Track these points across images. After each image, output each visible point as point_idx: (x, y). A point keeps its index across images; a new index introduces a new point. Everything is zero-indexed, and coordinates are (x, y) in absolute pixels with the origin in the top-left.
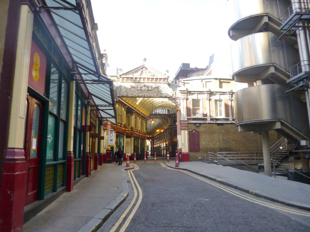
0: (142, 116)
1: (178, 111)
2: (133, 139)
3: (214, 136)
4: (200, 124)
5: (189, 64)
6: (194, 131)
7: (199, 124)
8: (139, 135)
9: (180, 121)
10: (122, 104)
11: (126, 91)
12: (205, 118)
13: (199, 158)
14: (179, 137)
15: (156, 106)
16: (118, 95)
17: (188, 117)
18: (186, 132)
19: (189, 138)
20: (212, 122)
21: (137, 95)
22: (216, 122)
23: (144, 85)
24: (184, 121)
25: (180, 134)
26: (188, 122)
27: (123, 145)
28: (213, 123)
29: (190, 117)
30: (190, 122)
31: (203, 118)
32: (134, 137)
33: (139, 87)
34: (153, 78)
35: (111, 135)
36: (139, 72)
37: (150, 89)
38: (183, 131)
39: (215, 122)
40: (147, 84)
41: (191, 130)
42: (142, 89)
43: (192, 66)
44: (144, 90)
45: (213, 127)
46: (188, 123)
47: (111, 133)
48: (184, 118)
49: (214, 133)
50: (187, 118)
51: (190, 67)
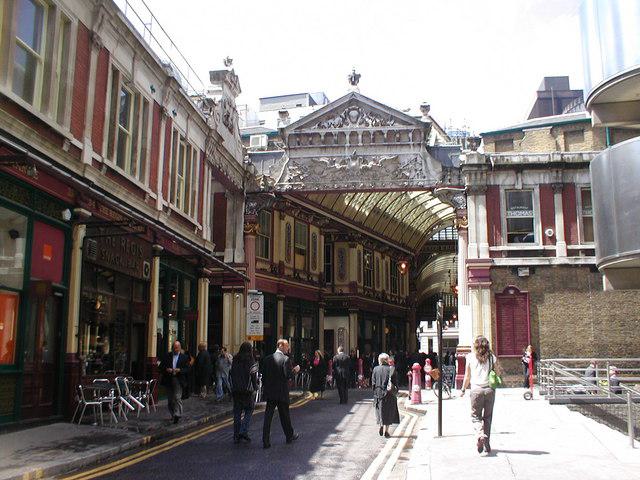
1: (462, 229)
4: (532, 268)
6: (512, 292)
9: (468, 261)
18: (487, 294)
28: (577, 266)
34: (381, 133)
35: (255, 306)
36: (338, 120)
40: (361, 152)
41: (501, 290)
44: (354, 168)
45: (576, 276)
46: (493, 267)
47: (257, 300)
48: (478, 252)
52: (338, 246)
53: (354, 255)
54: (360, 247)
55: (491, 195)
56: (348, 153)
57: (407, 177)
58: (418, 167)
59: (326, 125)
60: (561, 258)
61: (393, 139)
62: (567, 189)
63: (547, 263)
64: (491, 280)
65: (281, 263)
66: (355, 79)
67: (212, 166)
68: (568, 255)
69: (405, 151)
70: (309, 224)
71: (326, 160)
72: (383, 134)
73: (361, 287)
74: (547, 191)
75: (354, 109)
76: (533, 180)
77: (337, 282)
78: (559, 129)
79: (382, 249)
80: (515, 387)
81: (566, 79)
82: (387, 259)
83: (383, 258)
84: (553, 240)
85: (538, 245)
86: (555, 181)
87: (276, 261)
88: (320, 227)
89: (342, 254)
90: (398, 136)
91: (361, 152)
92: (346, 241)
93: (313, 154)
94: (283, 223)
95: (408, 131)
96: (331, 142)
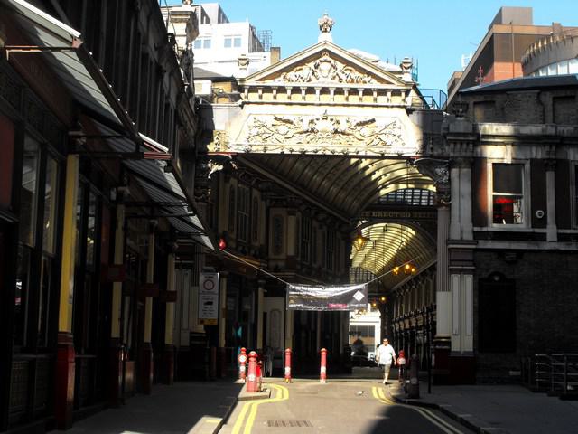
4: (520, 253)
6: (496, 279)
7: (513, 255)
9: (449, 241)
12: (537, 230)
13: (512, 373)
14: (442, 297)
17: (476, 229)
18: (469, 279)
19: (476, 300)
20: (562, 247)
24: (462, 241)
25: (448, 288)
26: (474, 246)
30: (483, 244)
31: (531, 230)
35: (209, 285)
38: (455, 278)
41: (485, 275)
46: (476, 250)
48: (462, 232)
50: (474, 232)
56: (317, 112)
57: (385, 144)
58: (396, 131)
62: (560, 166)
63: (536, 248)
64: (474, 265)
75: (326, 61)
77: (271, 255)
78: (548, 94)
80: (498, 384)
82: (325, 228)
84: (542, 222)
86: (548, 157)
92: (284, 207)
94: (228, 186)
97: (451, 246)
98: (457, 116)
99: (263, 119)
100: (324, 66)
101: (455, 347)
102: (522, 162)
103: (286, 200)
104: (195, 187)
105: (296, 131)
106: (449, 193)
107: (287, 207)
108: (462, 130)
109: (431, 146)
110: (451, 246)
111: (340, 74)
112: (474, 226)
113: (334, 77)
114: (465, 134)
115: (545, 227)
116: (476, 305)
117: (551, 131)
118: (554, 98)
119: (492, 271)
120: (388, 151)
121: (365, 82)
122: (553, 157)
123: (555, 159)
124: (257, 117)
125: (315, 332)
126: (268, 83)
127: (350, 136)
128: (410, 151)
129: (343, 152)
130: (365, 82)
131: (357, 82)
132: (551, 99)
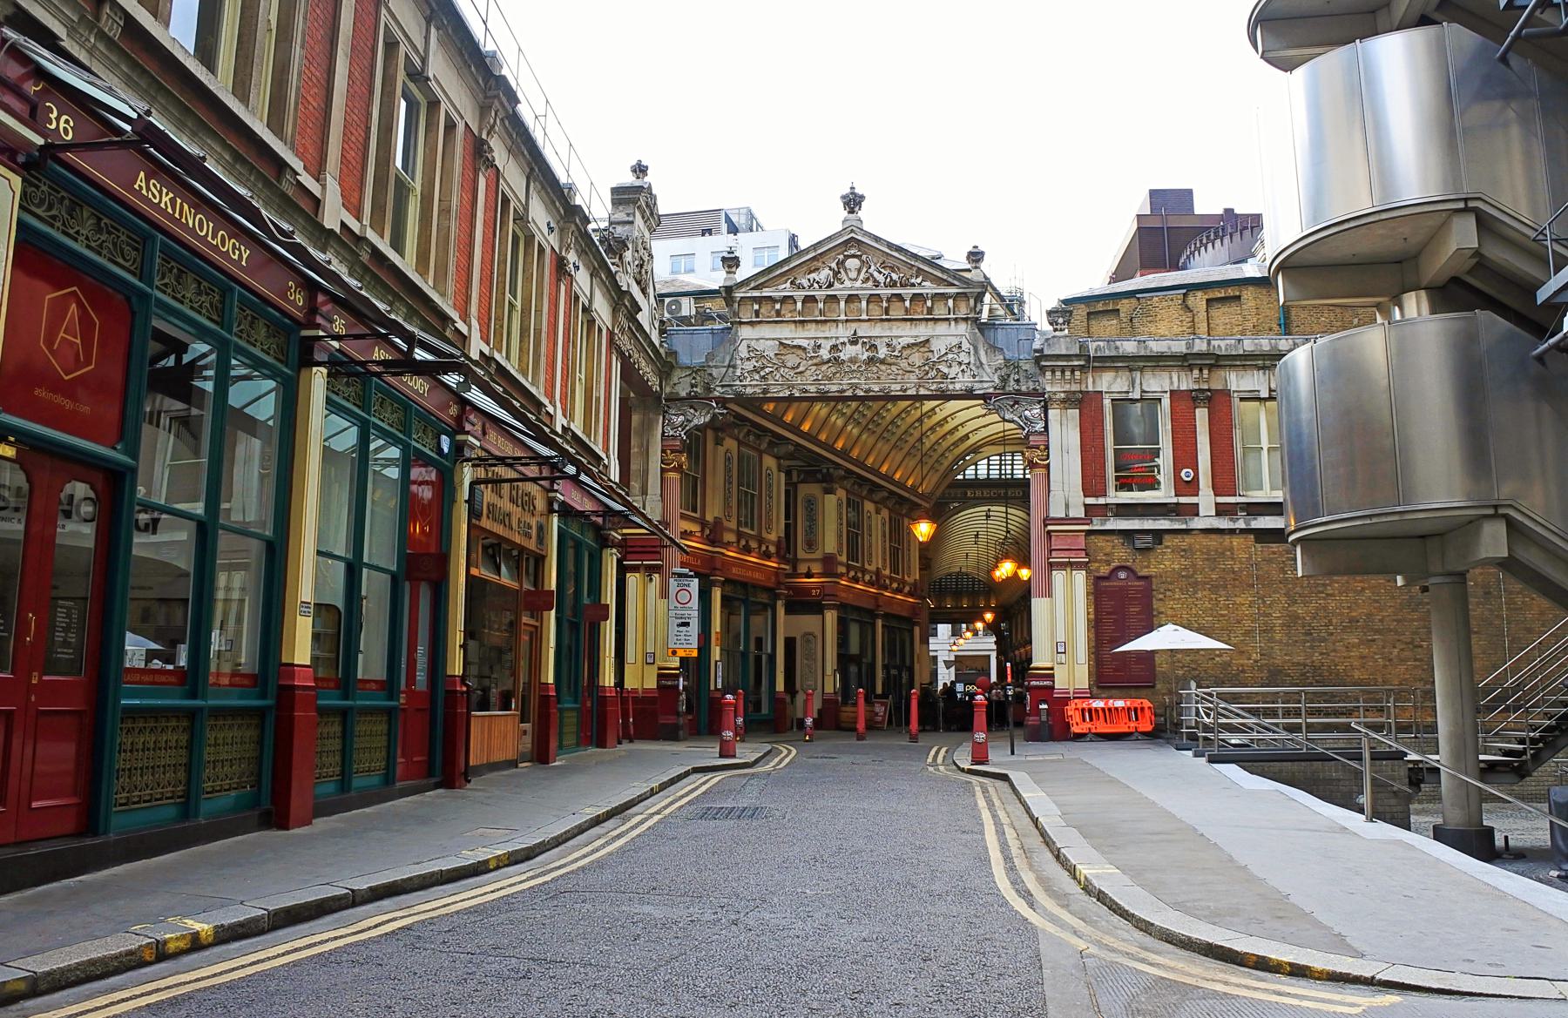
0: (892, 493)
2: (831, 617)
3: (1238, 600)
4: (1158, 535)
5: (1190, 192)
6: (1122, 575)
7: (1149, 538)
8: (876, 597)
9: (1047, 521)
10: (758, 437)
11: (756, 370)
12: (1183, 500)
15: (973, 439)
16: (719, 389)
18: (1080, 577)
20: (1224, 523)
21: (813, 389)
22: (1247, 523)
23: (849, 333)
24: (1067, 520)
27: (769, 651)
28: (1232, 531)
29: (1101, 501)
31: (1175, 500)
32: (842, 608)
33: (827, 345)
34: (900, 298)
35: (684, 597)
36: (824, 275)
37: (883, 352)
38: (1058, 577)
39: (1241, 524)
40: (864, 330)
41: (1104, 570)
42: (841, 354)
43: (1206, 205)
44: (853, 360)
45: (1231, 549)
48: (1067, 506)
49: (1234, 586)
50: (1086, 506)
51: (1197, 212)
52: (804, 490)
53: (831, 506)
54: (841, 493)
55: (1086, 403)
56: (843, 332)
57: (945, 376)
58: (964, 358)
59: (805, 283)
60: (1207, 519)
61: (921, 309)
63: (1184, 527)
65: (717, 521)
66: (853, 202)
67: (621, 354)
68: (1218, 514)
69: (941, 328)
70: (761, 453)
71: (804, 343)
72: (904, 300)
73: (841, 564)
74: (1184, 402)
75: (853, 256)
76: (1158, 383)
77: (801, 554)
78: (1199, 294)
79: (879, 496)
81: (1188, 194)
82: (885, 513)
83: (878, 512)
84: (1192, 487)
85: (1163, 494)
86: (1196, 387)
87: (709, 518)
88: (778, 458)
89: (811, 504)
90: (929, 303)
91: (864, 330)
92: (818, 481)
93: (786, 333)
95: (944, 297)
96: (814, 310)
97: (1050, 528)
98: (1055, 330)
99: (760, 346)
100: (852, 263)
101: (1060, 683)
102: (1157, 395)
103: (820, 471)
104: (663, 451)
105: (810, 362)
106: (1047, 448)
107: (822, 482)
108: (1064, 352)
109: (1016, 377)
110: (1050, 528)
111: (876, 274)
112: (1085, 496)
113: (868, 279)
114: (1068, 357)
115: (1197, 495)
116: (1092, 617)
117: (1200, 346)
118: (1208, 300)
119: (1114, 565)
120: (951, 387)
121: (913, 285)
122: (1206, 387)
123: (1209, 390)
124: (753, 343)
125: (872, 666)
126: (766, 292)
127: (894, 368)
128: (986, 385)
129: (881, 391)
130: (913, 285)
131: (901, 286)
132: (1204, 302)
